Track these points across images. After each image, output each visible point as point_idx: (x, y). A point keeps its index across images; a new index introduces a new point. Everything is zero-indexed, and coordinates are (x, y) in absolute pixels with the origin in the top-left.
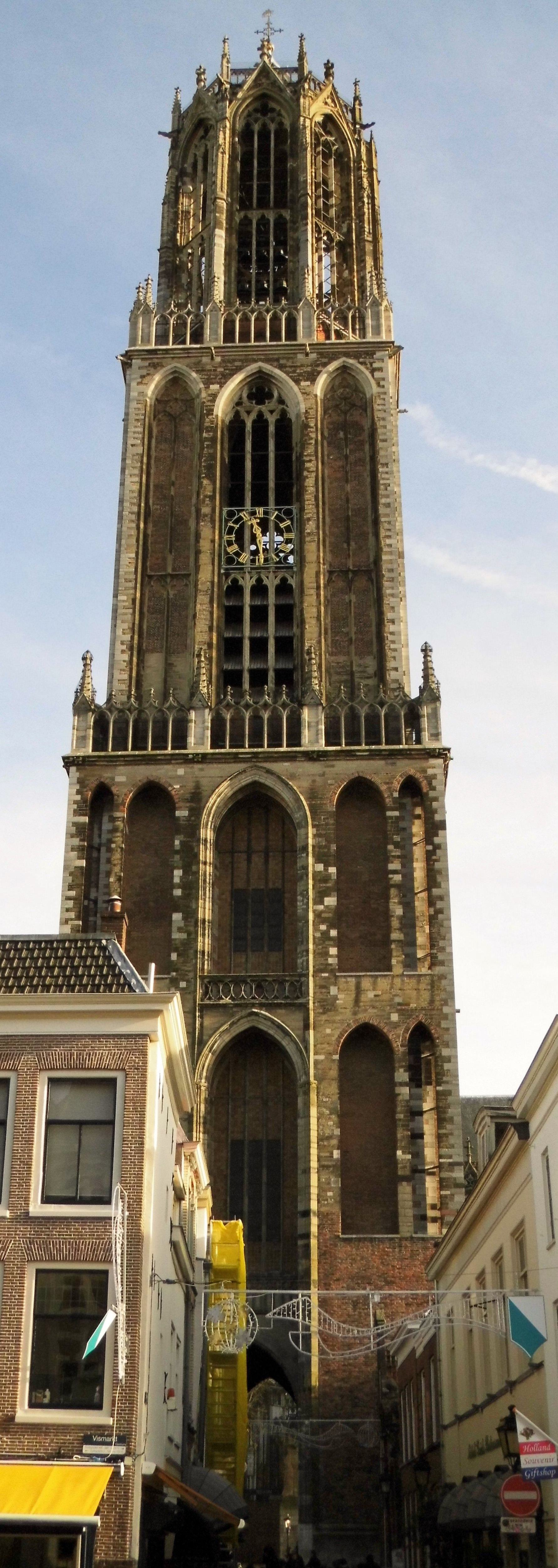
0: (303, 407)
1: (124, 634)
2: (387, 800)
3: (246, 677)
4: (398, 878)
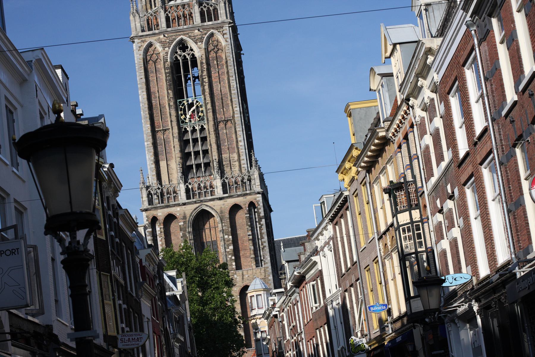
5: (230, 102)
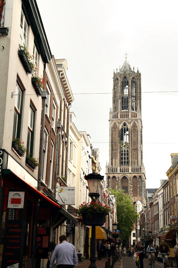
0: (129, 127)
4: (138, 187)
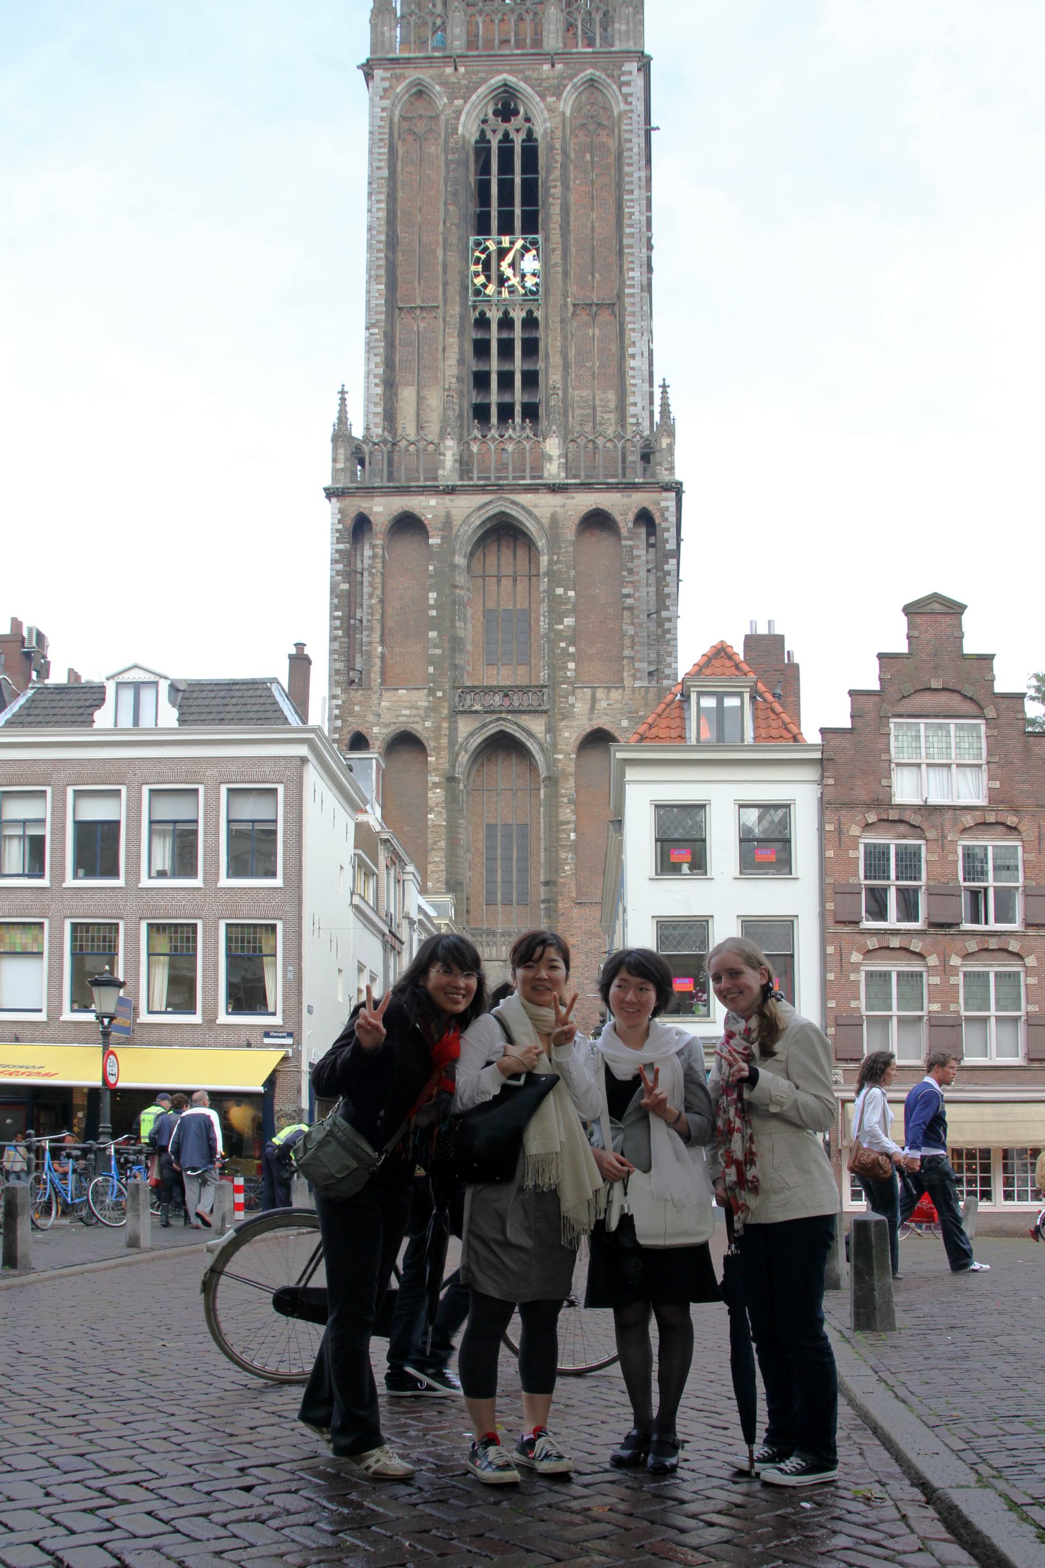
1: (376, 367)
2: (623, 531)
3: (494, 411)
5: (614, 259)
